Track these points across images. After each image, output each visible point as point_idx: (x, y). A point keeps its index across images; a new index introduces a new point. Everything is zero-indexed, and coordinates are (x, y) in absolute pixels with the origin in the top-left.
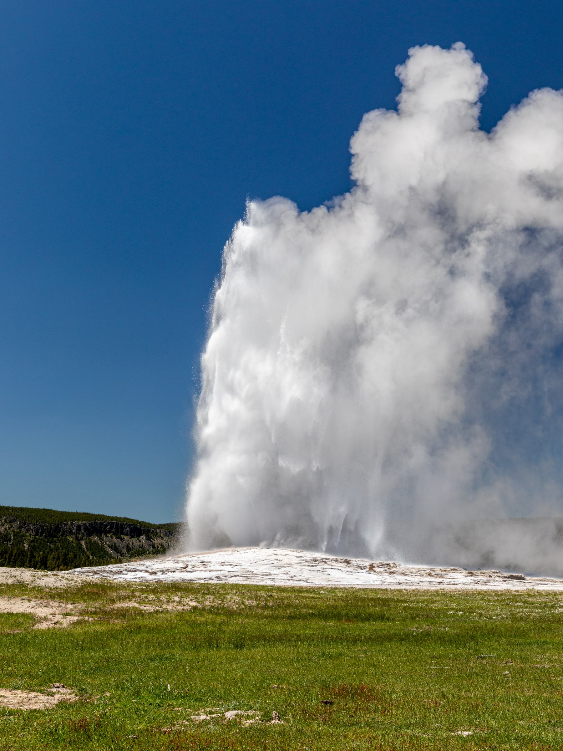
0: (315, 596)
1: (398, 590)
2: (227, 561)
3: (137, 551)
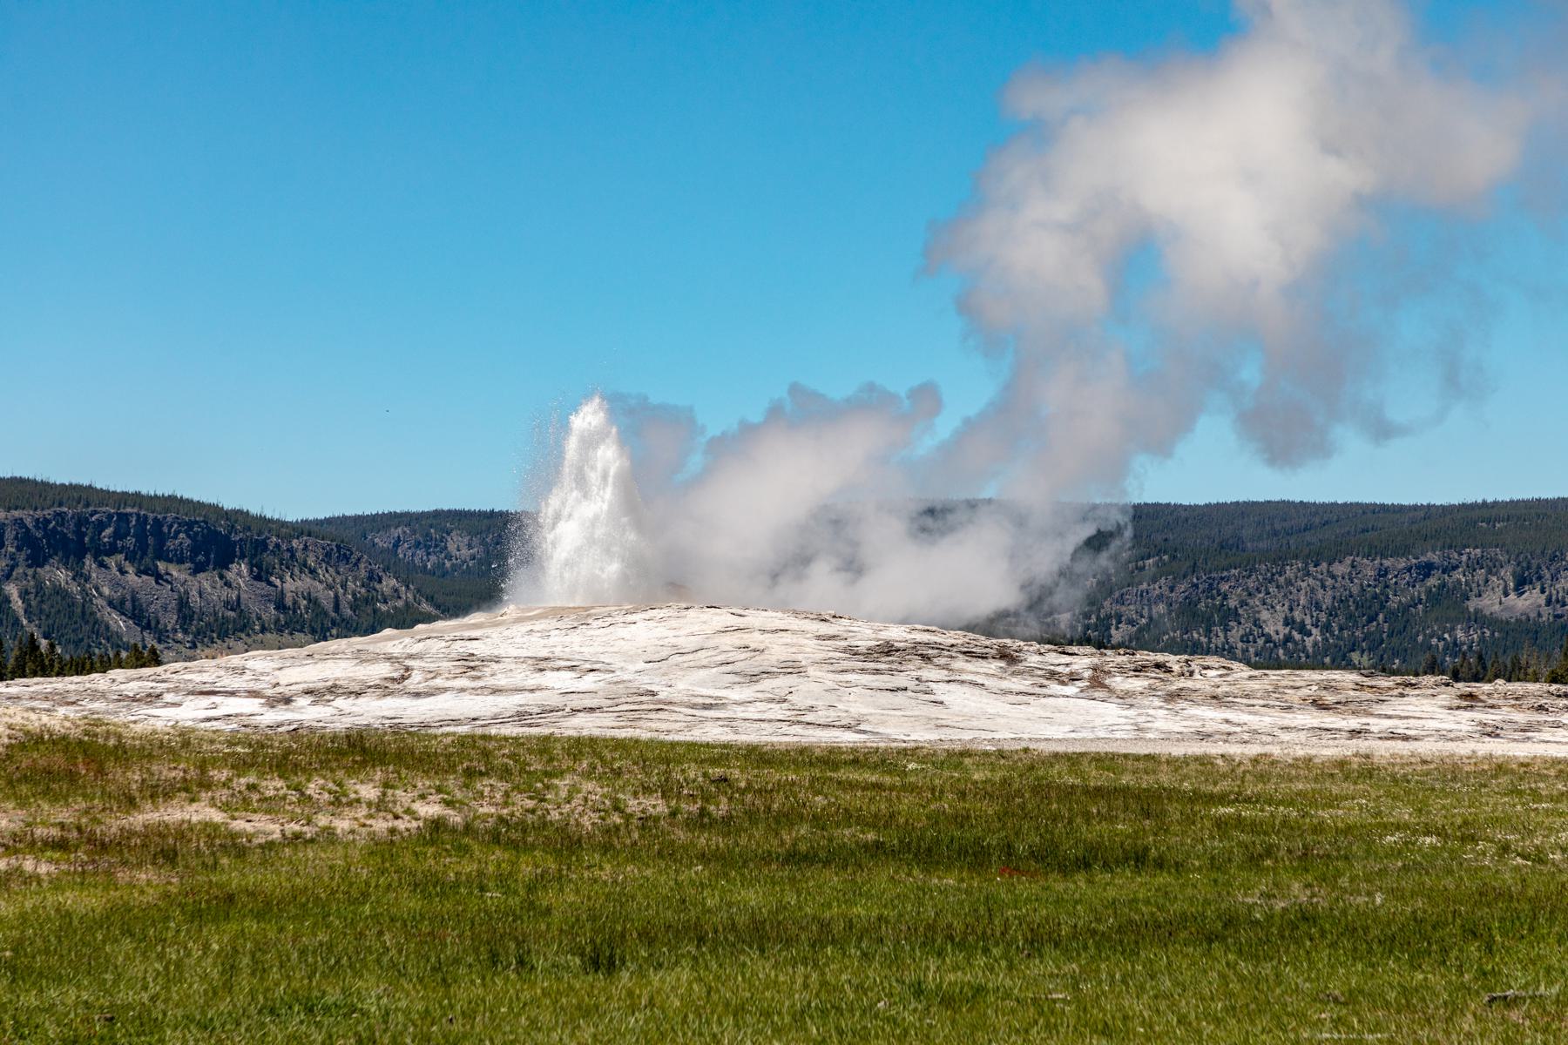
0: (887, 780)
1: (1197, 759)
2: (558, 652)
3: (216, 620)
